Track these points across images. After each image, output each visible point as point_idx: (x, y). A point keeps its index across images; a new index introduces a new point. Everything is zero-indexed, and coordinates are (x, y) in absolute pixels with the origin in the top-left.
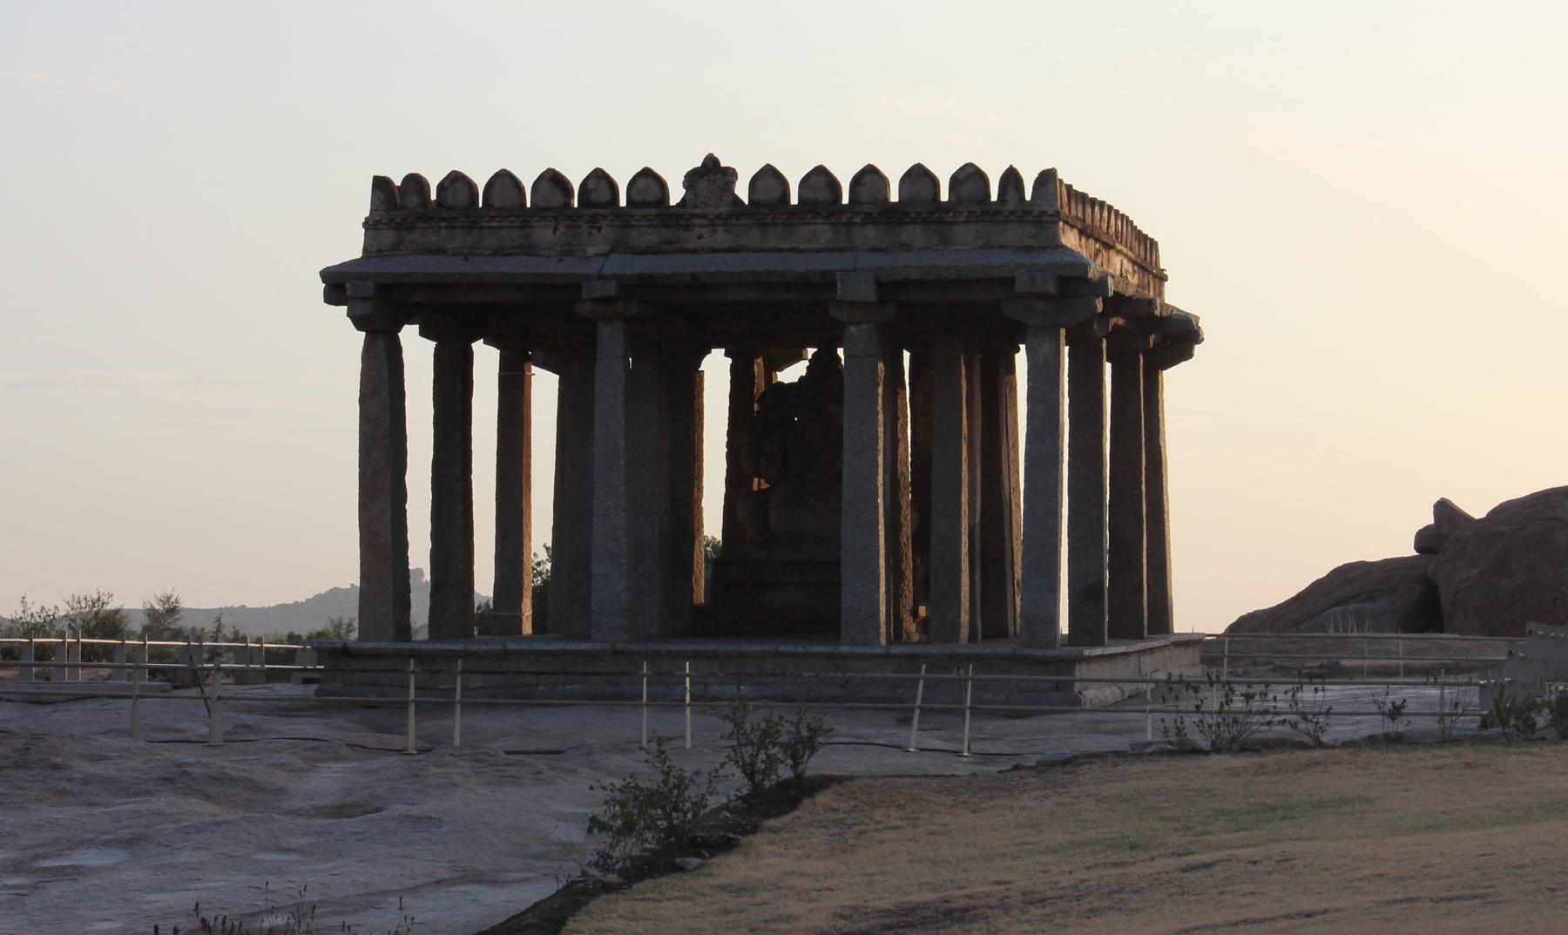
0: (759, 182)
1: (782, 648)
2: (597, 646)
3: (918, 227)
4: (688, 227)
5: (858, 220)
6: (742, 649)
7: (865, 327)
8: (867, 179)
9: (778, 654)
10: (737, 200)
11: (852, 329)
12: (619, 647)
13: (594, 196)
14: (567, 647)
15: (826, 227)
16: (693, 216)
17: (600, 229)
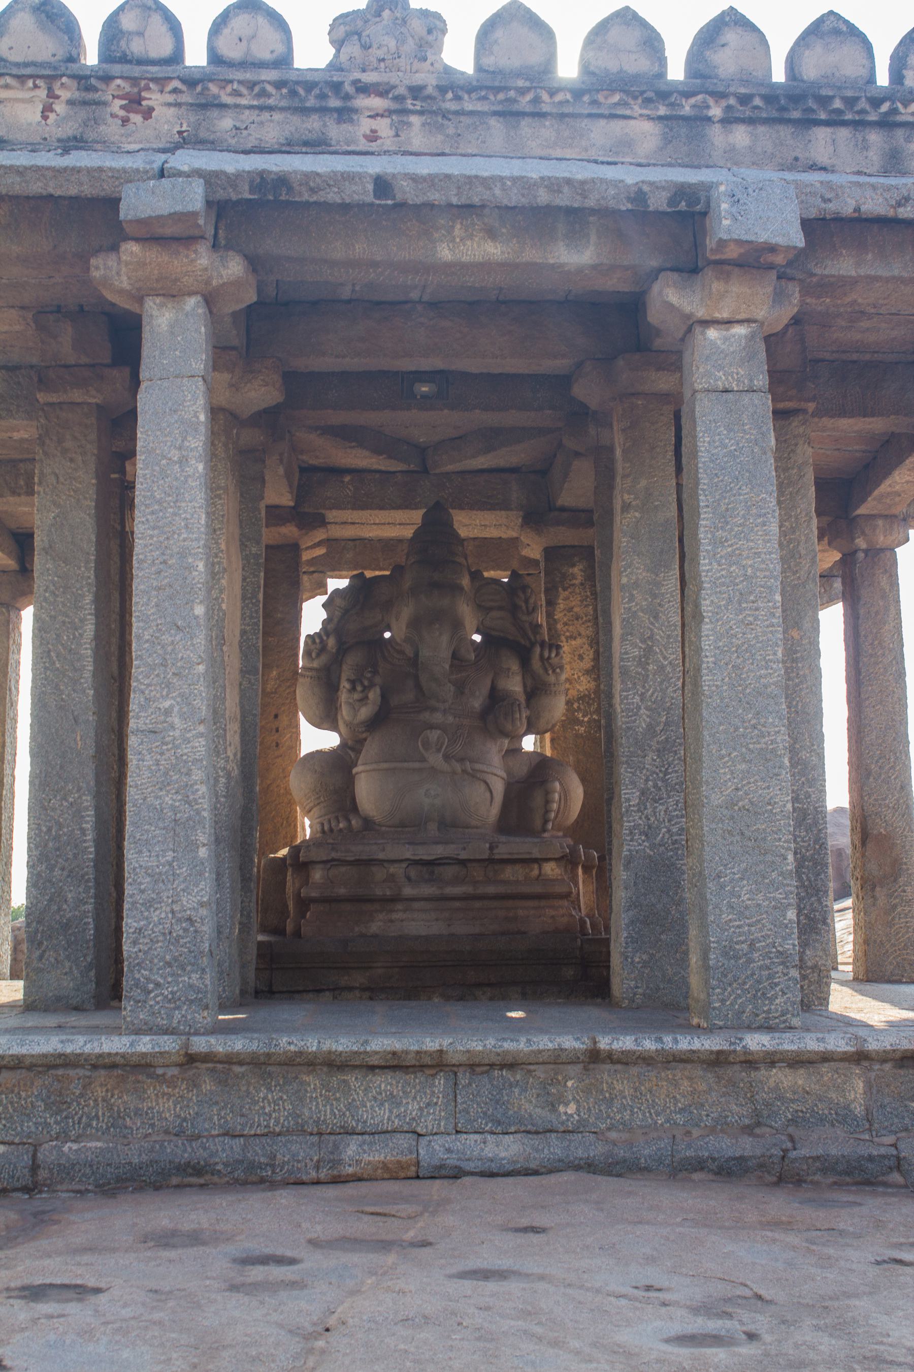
0: (499, 34)
1: (604, 1043)
2: (145, 1045)
3: (844, 133)
4: (345, 114)
5: (716, 112)
6: (508, 1045)
7: (740, 330)
8: (731, 36)
9: (595, 1057)
10: (448, 70)
11: (712, 334)
12: (200, 1044)
13: (136, 47)
14: (69, 1049)
15: (647, 126)
16: (364, 89)
17: (148, 113)
